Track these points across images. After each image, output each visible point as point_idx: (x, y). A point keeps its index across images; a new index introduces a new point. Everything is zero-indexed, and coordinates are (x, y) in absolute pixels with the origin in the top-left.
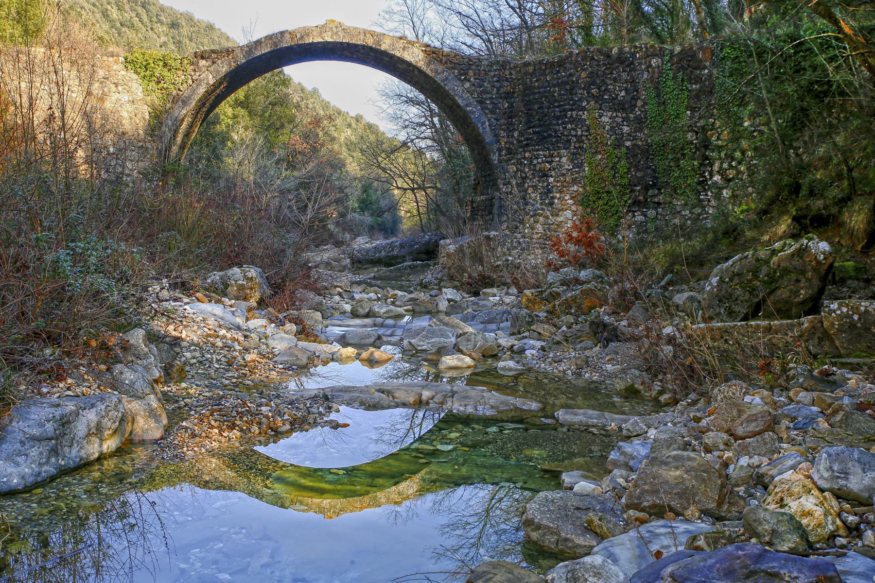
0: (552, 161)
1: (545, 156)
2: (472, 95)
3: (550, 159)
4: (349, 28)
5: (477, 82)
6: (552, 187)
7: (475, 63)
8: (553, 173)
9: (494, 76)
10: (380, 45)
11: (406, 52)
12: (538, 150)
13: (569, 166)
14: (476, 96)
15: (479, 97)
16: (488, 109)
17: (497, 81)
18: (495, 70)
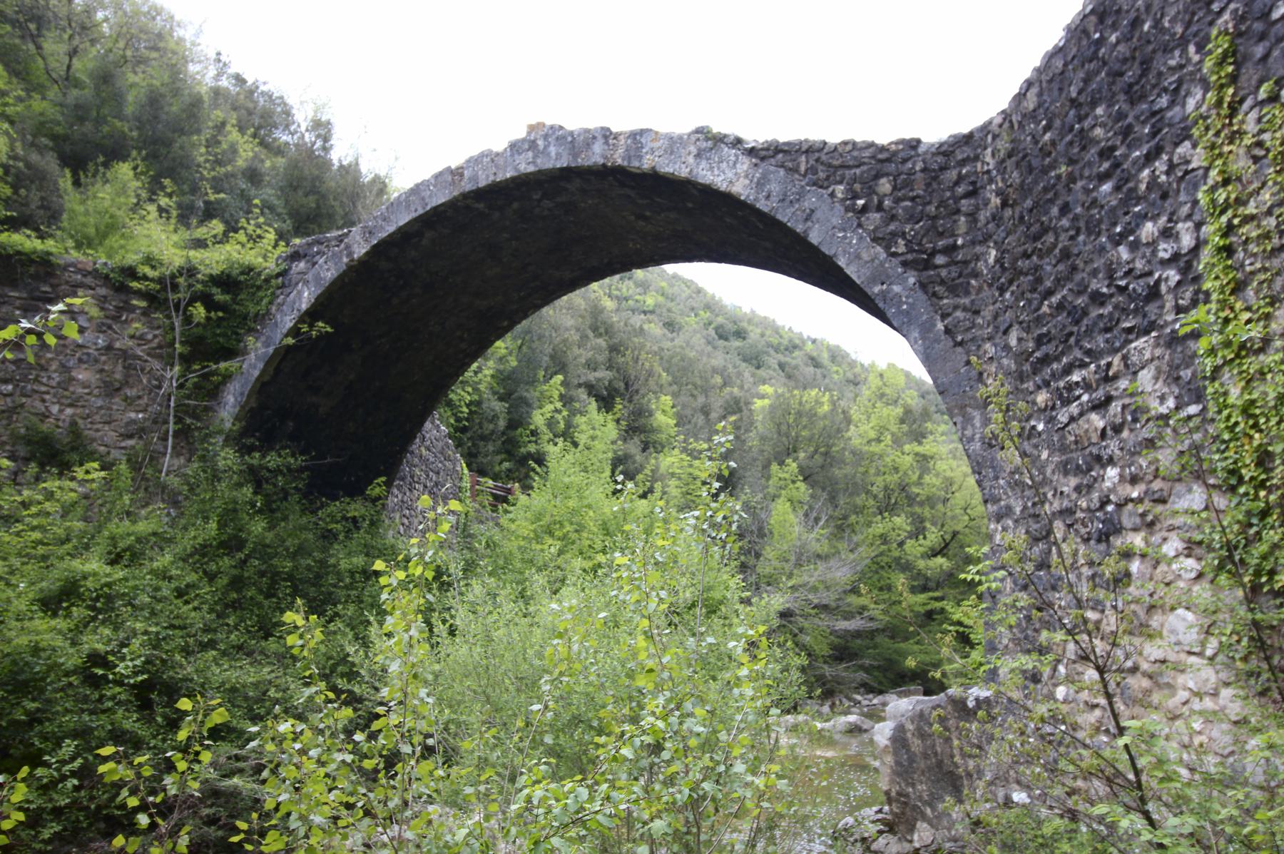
0: (1109, 399)
1: (1087, 386)
2: (887, 248)
3: (1100, 394)
4: (571, 133)
5: (905, 209)
6: (1120, 506)
7: (895, 153)
8: (1113, 446)
9: (960, 179)
10: (640, 158)
11: (704, 164)
12: (1068, 370)
13: (1162, 399)
14: (902, 249)
15: (911, 251)
16: (942, 282)
17: (968, 195)
18: (963, 162)
